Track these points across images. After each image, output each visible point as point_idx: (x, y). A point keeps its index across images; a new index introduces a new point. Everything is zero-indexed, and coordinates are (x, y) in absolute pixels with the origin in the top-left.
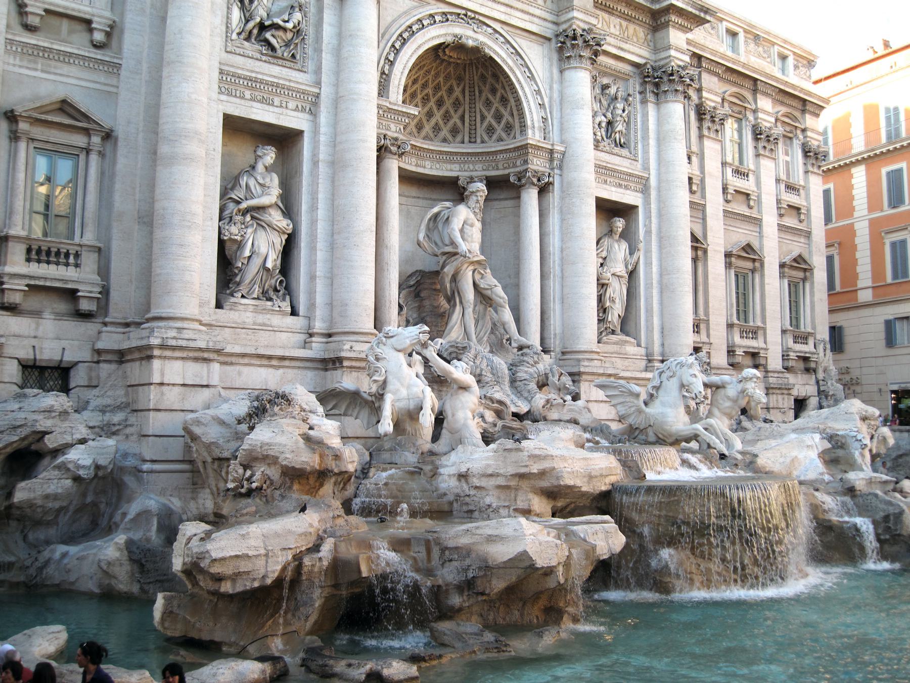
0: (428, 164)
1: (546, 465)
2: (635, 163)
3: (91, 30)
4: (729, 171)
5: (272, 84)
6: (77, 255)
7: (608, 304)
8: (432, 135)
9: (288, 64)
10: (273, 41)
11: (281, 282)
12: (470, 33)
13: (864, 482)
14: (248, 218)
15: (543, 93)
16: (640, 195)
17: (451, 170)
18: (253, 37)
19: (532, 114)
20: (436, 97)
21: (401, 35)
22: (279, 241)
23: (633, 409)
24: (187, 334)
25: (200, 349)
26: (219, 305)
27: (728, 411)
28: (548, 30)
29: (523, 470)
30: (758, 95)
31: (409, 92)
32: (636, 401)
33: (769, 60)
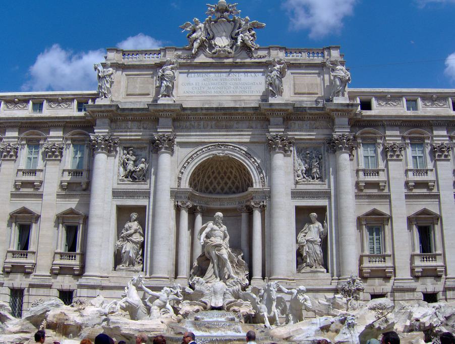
0: (226, 203)
3: (81, 186)
4: (410, 174)
6: (75, 257)
7: (304, 254)
8: (228, 191)
9: (140, 183)
11: (141, 260)
13: (310, 342)
15: (261, 166)
19: (255, 177)
21: (187, 161)
24: (89, 281)
28: (264, 140)
30: (434, 128)
31: (212, 177)
33: (445, 106)
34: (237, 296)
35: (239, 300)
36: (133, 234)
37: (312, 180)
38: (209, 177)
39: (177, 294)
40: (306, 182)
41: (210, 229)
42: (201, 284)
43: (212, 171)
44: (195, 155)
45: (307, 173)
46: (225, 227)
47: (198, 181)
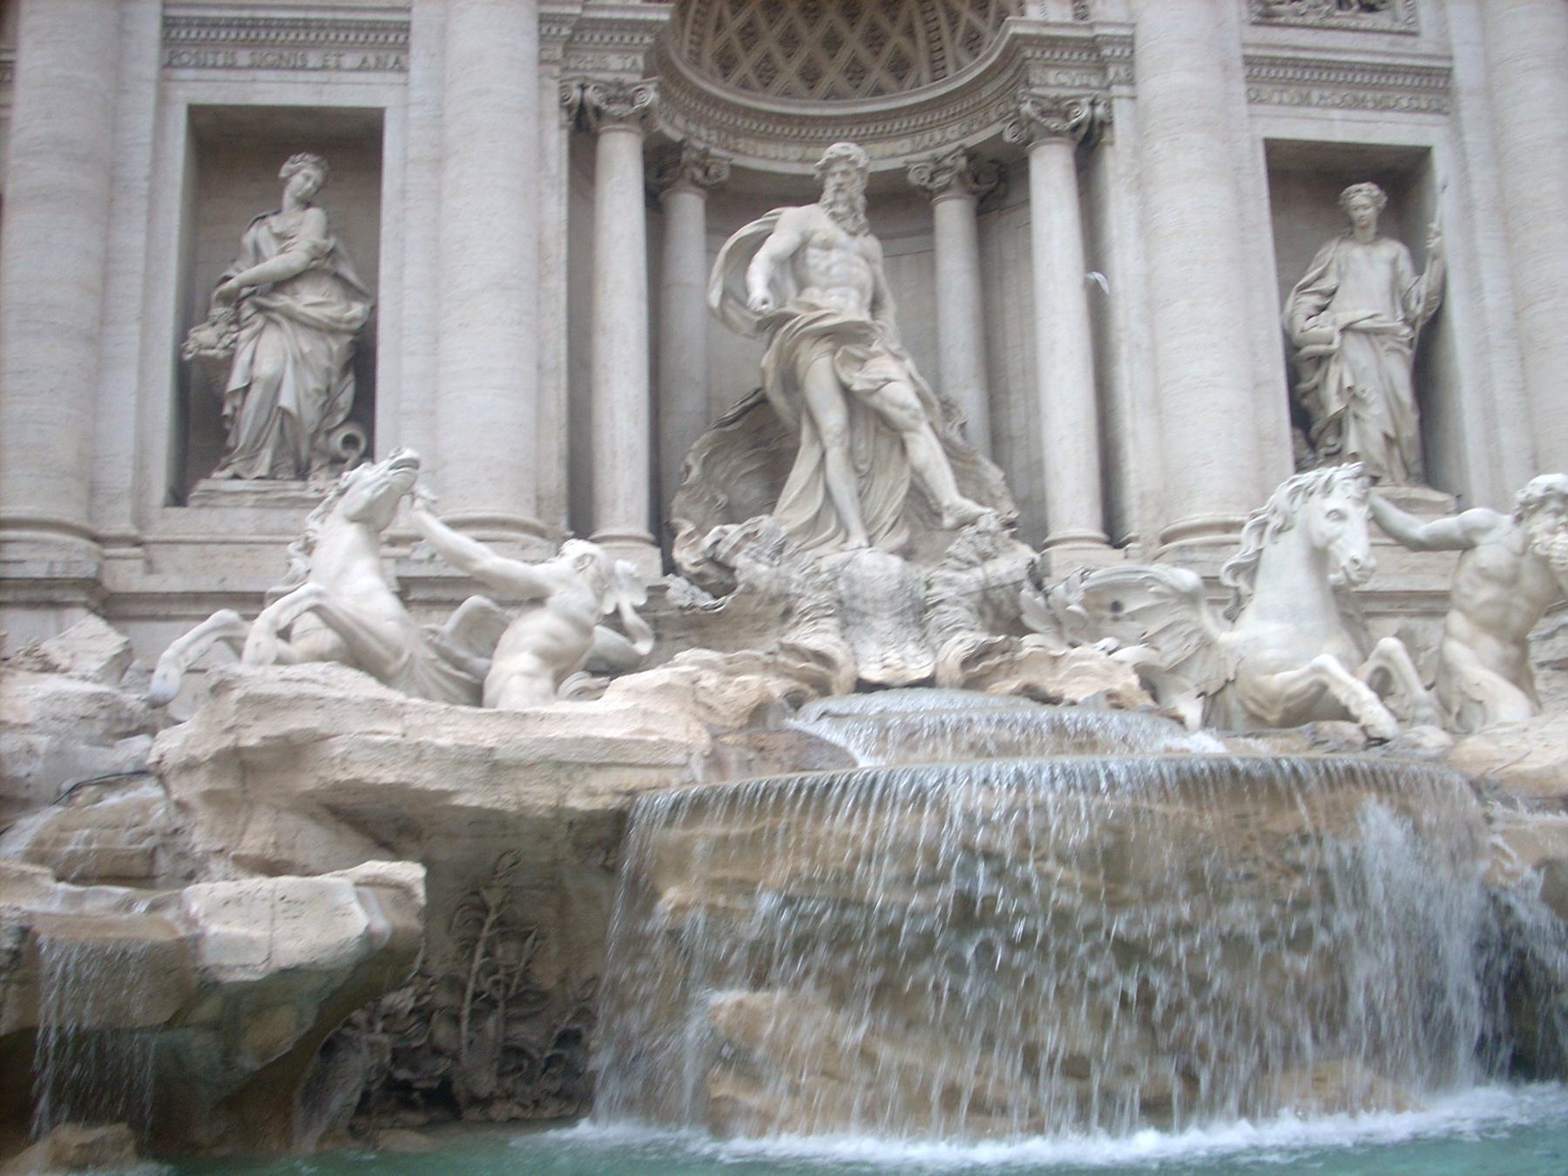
1: (293, 723)
2: (1410, 40)
5: (294, 25)
7: (1335, 406)
8: (843, 84)
11: (350, 441)
14: (247, 311)
16: (1430, 118)
17: (893, 156)
22: (327, 353)
23: (1194, 640)
25: (36, 583)
26: (178, 497)
27: (1491, 614)
29: (228, 741)
32: (1195, 619)
34: (1002, 615)
35: (1028, 640)
37: (1338, 13)
39: (614, 620)
40: (1311, 19)
42: (780, 550)
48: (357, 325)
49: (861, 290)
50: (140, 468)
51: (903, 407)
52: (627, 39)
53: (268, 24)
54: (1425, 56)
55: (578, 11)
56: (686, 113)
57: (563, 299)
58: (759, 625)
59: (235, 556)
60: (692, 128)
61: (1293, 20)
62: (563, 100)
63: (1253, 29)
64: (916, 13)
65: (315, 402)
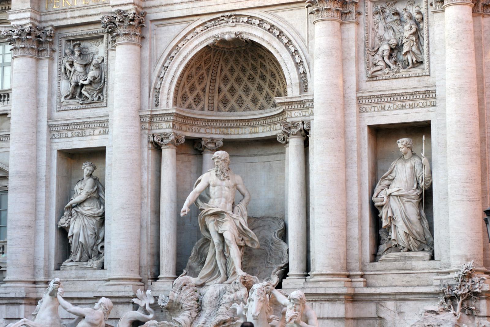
0: (260, 129)
2: (427, 78)
5: (81, 123)
7: (384, 224)
8: (265, 104)
10: (85, 93)
12: (228, 29)
14: (73, 212)
15: (300, 52)
16: (431, 109)
18: (78, 94)
19: (291, 74)
20: (258, 75)
21: (169, 55)
24: (8, 290)
25: (13, 298)
31: (232, 81)
36: (84, 201)
37: (401, 70)
38: (226, 80)
41: (206, 184)
43: (229, 67)
44: (182, 43)
45: (394, 54)
46: (238, 179)
47: (204, 90)
48: (101, 214)
49: (226, 198)
50: (47, 259)
51: (227, 240)
52: (166, 119)
53: (74, 124)
54: (425, 87)
55: (150, 113)
56: (205, 127)
57: (150, 204)
58: (178, 310)
59: (70, 285)
60: (208, 131)
61: (381, 78)
62: (149, 141)
63: (368, 83)
64: (279, 79)
65: (91, 237)
